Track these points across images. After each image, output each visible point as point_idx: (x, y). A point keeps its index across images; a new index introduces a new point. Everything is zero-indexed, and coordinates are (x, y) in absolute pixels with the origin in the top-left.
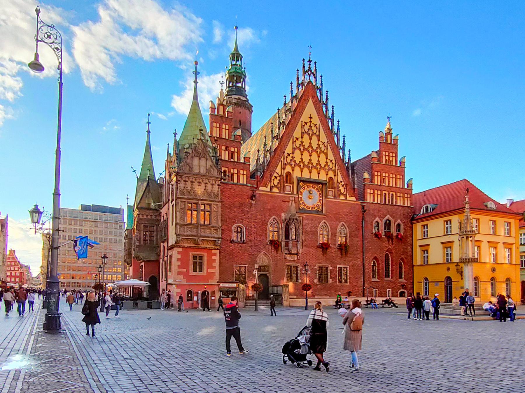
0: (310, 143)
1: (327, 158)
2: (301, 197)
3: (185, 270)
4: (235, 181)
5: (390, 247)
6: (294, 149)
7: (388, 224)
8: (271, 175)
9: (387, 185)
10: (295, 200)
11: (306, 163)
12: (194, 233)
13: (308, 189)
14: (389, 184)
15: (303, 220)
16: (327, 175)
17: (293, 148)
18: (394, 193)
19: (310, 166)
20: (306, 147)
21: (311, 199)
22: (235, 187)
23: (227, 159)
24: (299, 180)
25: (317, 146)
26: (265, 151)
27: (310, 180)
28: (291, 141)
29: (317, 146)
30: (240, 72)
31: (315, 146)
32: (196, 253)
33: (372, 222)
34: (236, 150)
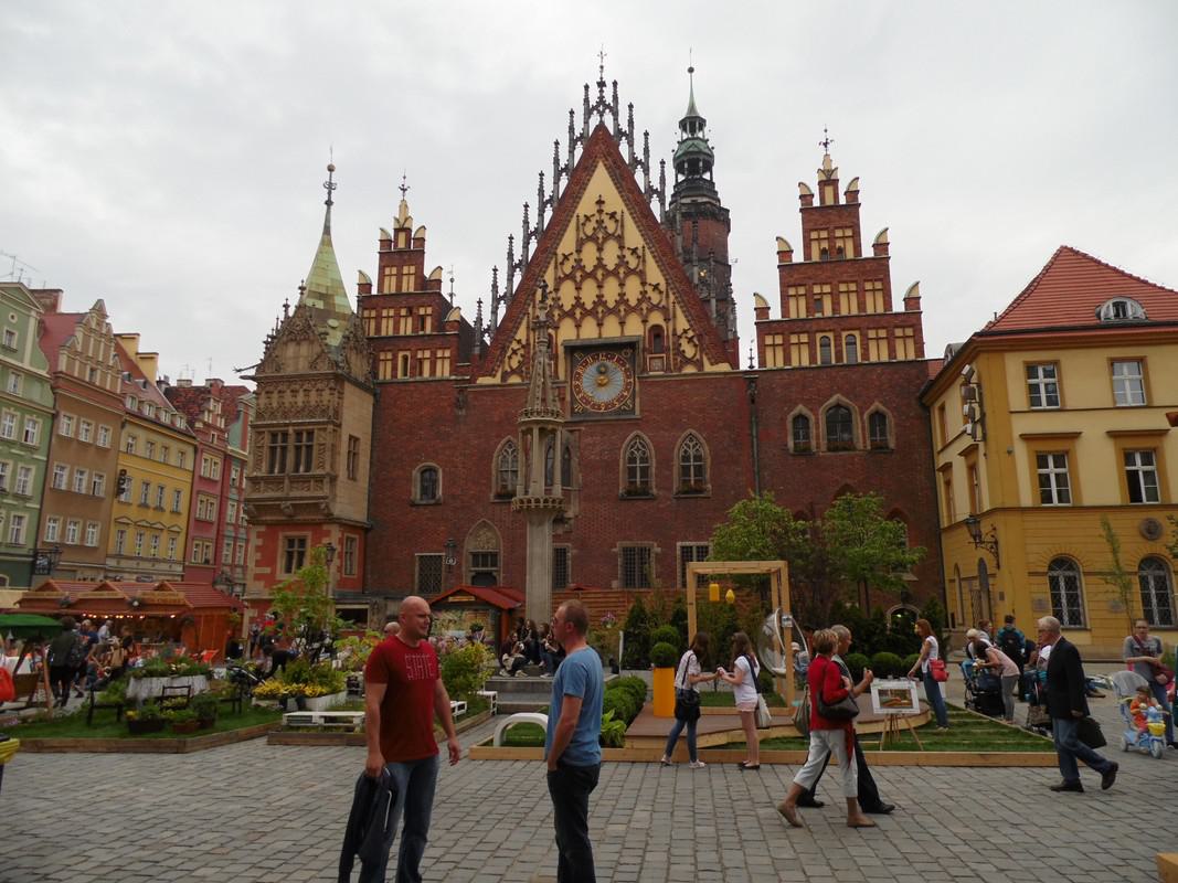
0: (600, 259)
1: (644, 283)
2: (578, 386)
3: (267, 570)
4: (426, 374)
5: (849, 481)
6: (559, 281)
7: (839, 420)
8: (504, 349)
9: (828, 312)
10: (559, 394)
11: (589, 306)
12: (278, 494)
13: (596, 365)
14: (834, 310)
15: (580, 437)
16: (645, 321)
17: (556, 279)
18: (857, 333)
19: (599, 311)
20: (589, 269)
21: (605, 388)
22: (421, 386)
23: (409, 333)
24: (571, 350)
25: (617, 261)
26: (496, 300)
27: (601, 341)
28: (552, 267)
29: (617, 261)
30: (696, 149)
31: (610, 260)
32: (289, 533)
33: (783, 420)
34: (429, 310)
